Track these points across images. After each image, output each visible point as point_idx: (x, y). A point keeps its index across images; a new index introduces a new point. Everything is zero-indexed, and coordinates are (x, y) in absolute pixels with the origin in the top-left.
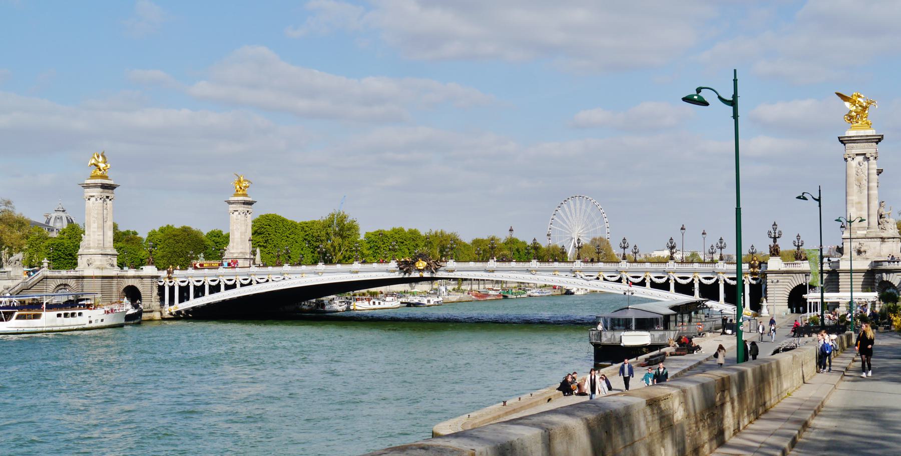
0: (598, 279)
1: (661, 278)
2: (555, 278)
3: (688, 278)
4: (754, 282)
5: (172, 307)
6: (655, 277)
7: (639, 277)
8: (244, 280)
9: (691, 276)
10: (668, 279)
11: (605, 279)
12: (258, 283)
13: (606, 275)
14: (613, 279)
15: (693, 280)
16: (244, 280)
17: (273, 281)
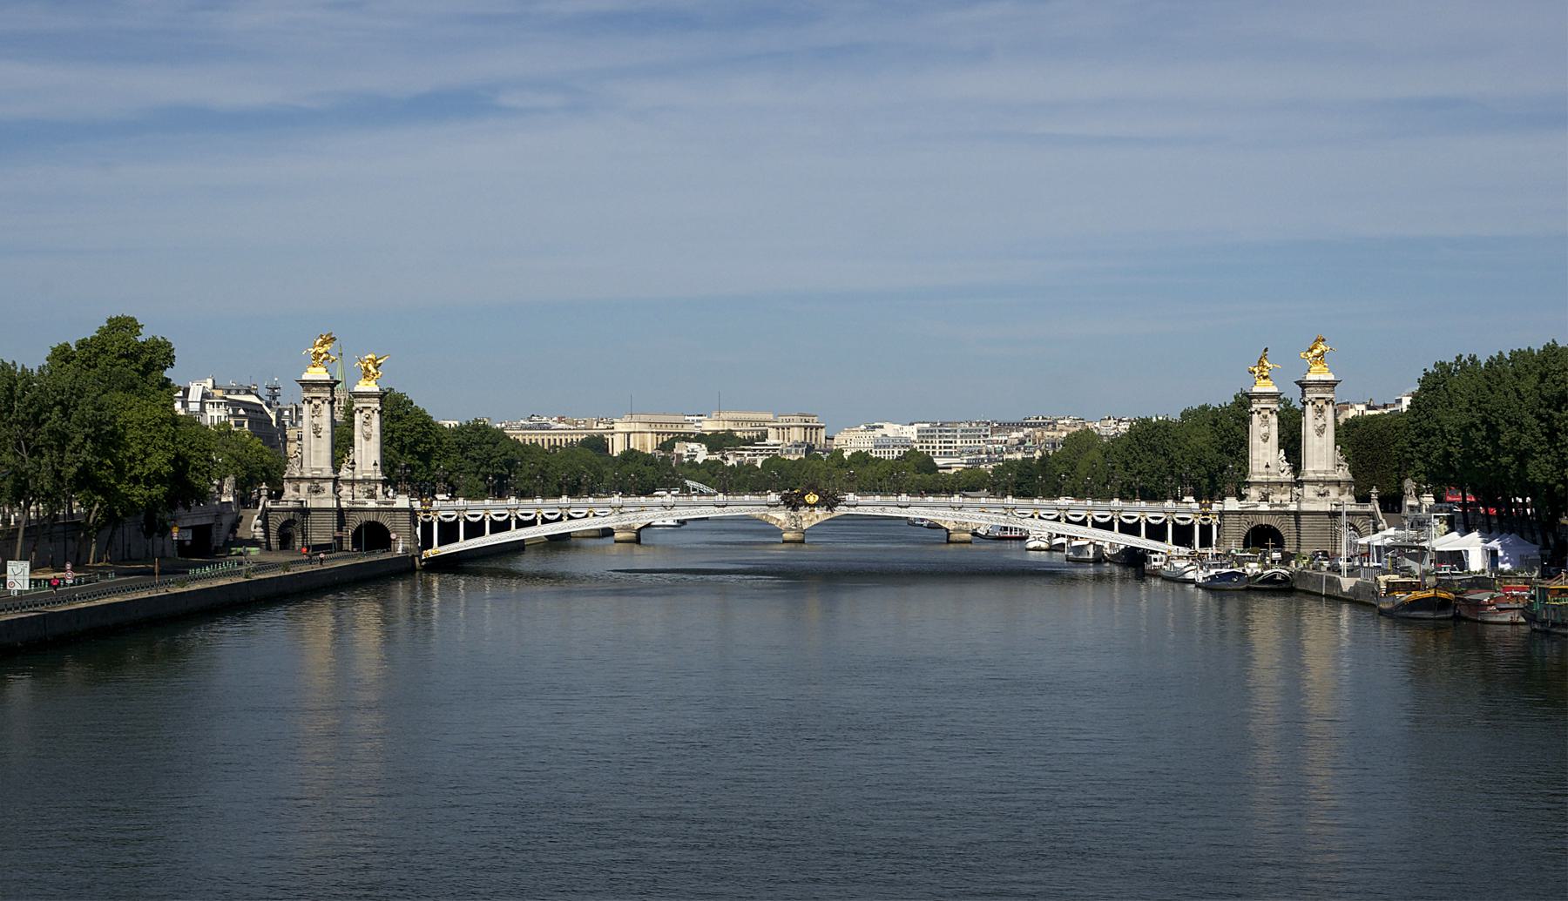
0: (1032, 517)
1: (1105, 517)
2: (984, 515)
3: (1133, 518)
4: (1205, 523)
5: (429, 551)
6: (1098, 516)
7: (1080, 516)
8: (549, 514)
9: (1137, 515)
10: (1112, 519)
11: (1040, 517)
12: (570, 518)
13: (1042, 513)
14: (1050, 517)
15: (1140, 519)
16: (549, 514)
17: (595, 515)
